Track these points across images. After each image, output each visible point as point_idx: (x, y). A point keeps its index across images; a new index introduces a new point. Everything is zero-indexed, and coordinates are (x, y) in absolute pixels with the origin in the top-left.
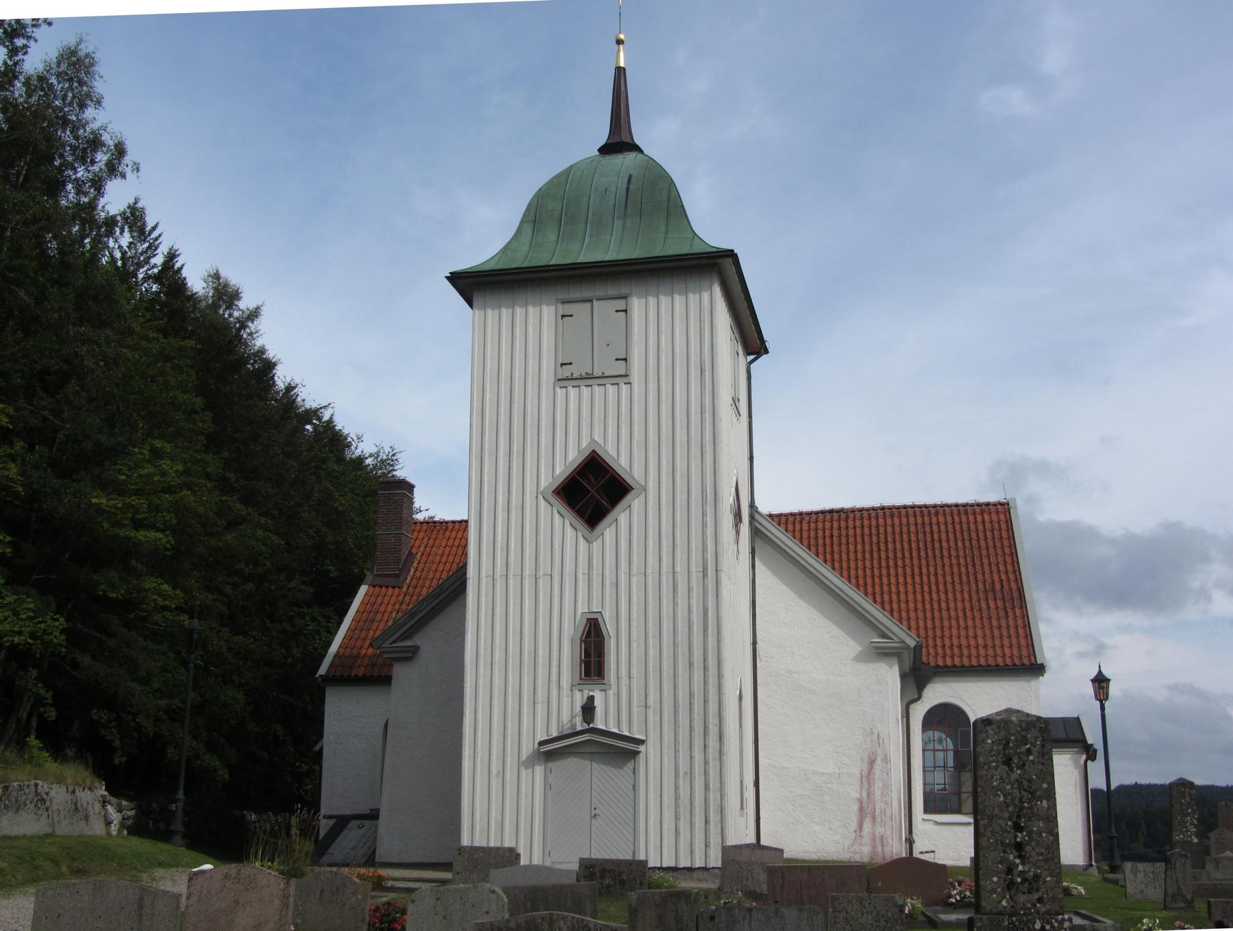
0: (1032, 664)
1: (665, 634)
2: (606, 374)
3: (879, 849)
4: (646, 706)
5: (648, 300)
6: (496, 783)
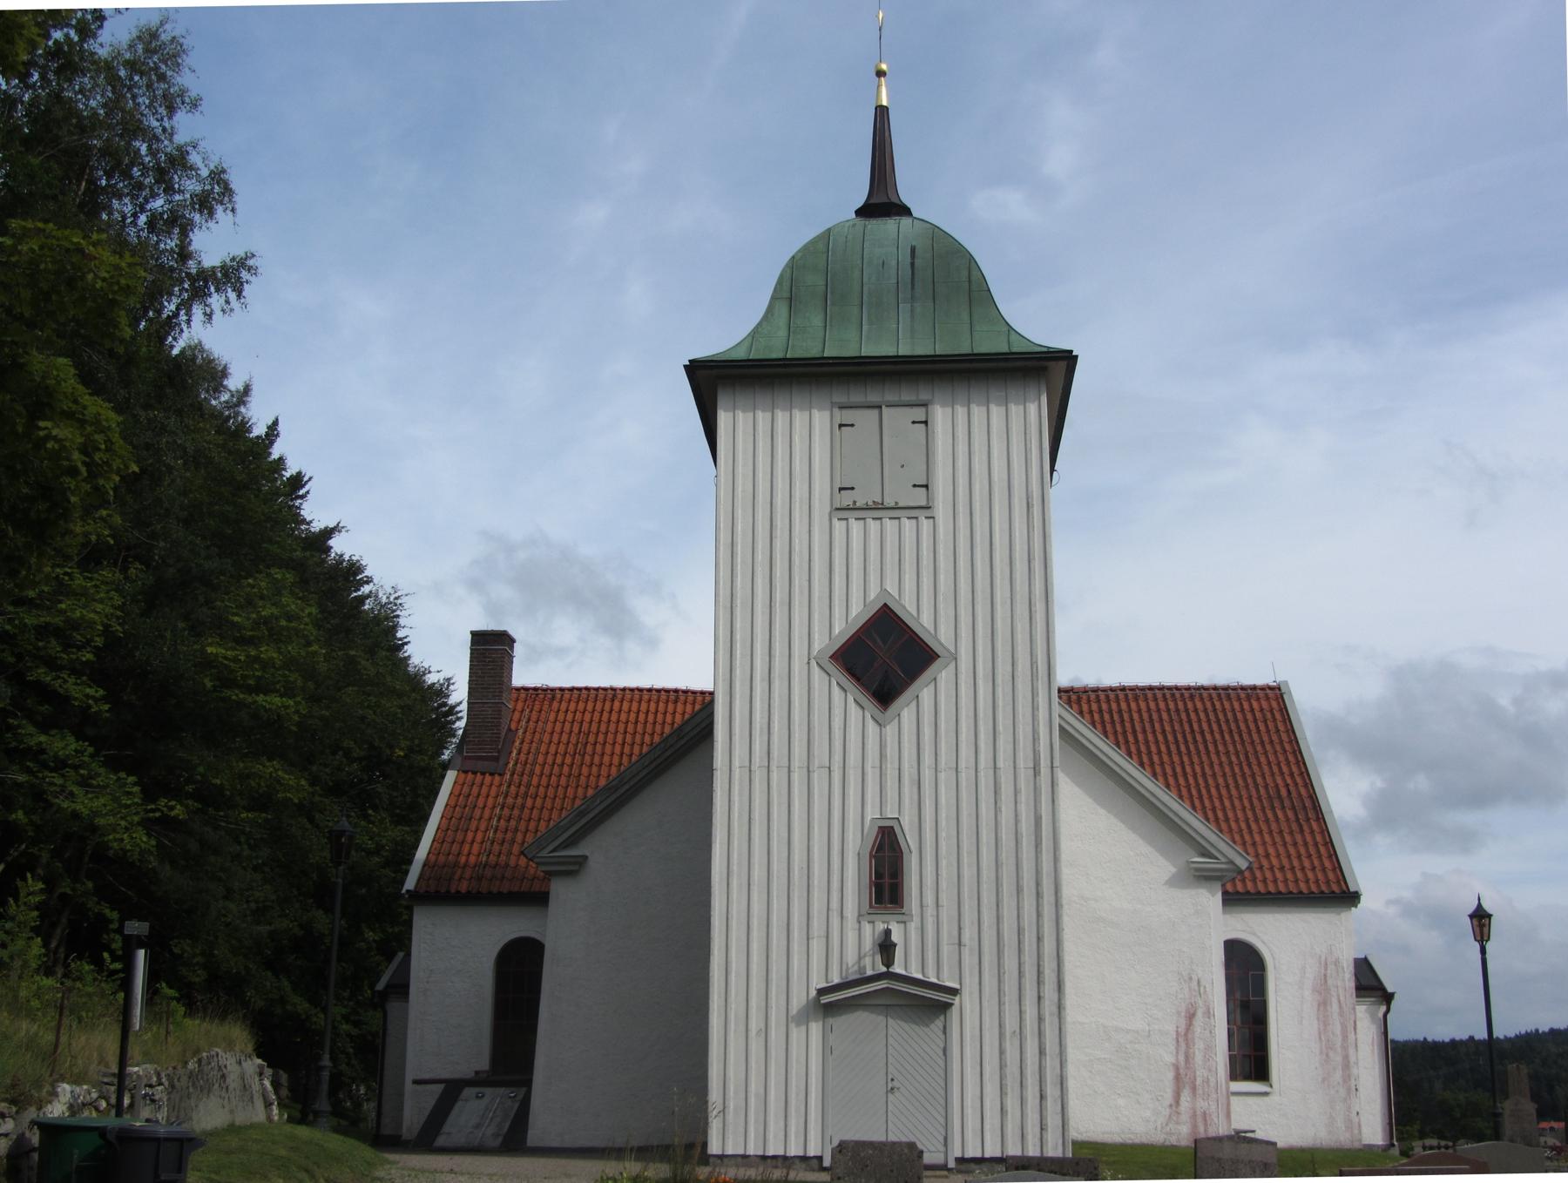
0: (1344, 892)
1: (984, 850)
2: (900, 505)
3: (1201, 1129)
4: (960, 944)
5: (955, 410)
6: (756, 1046)
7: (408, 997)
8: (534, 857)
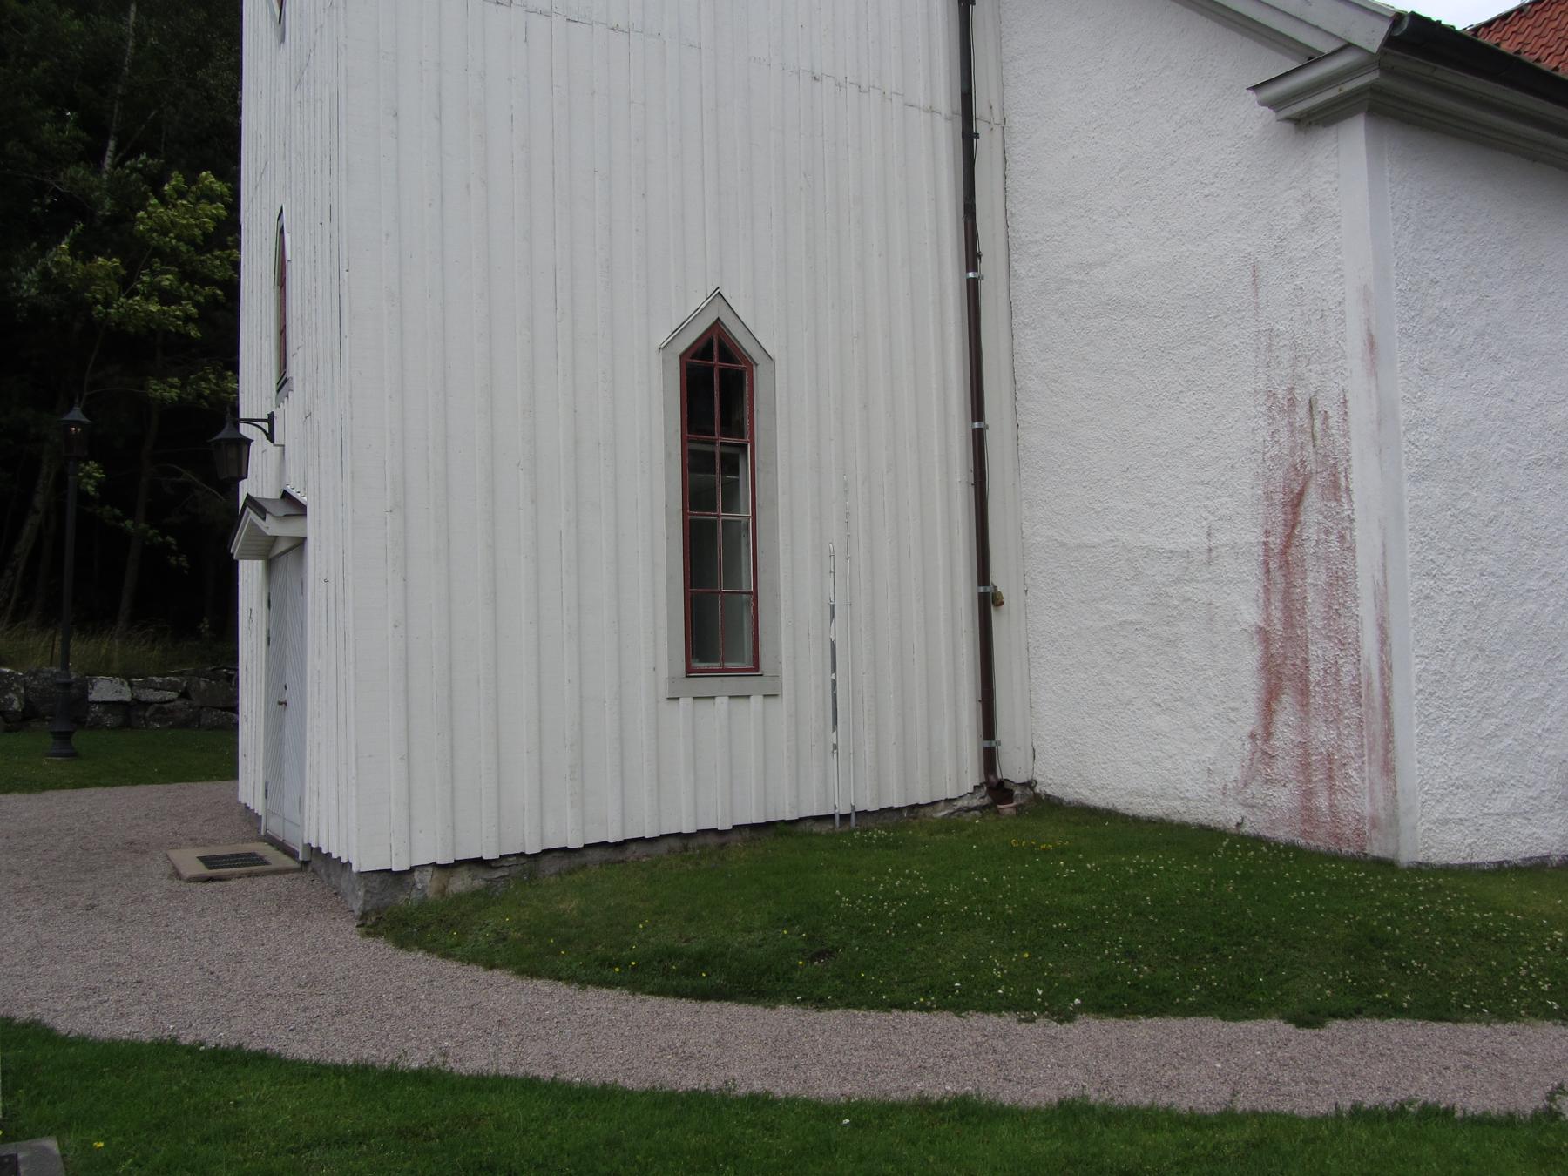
3: (1322, 802)
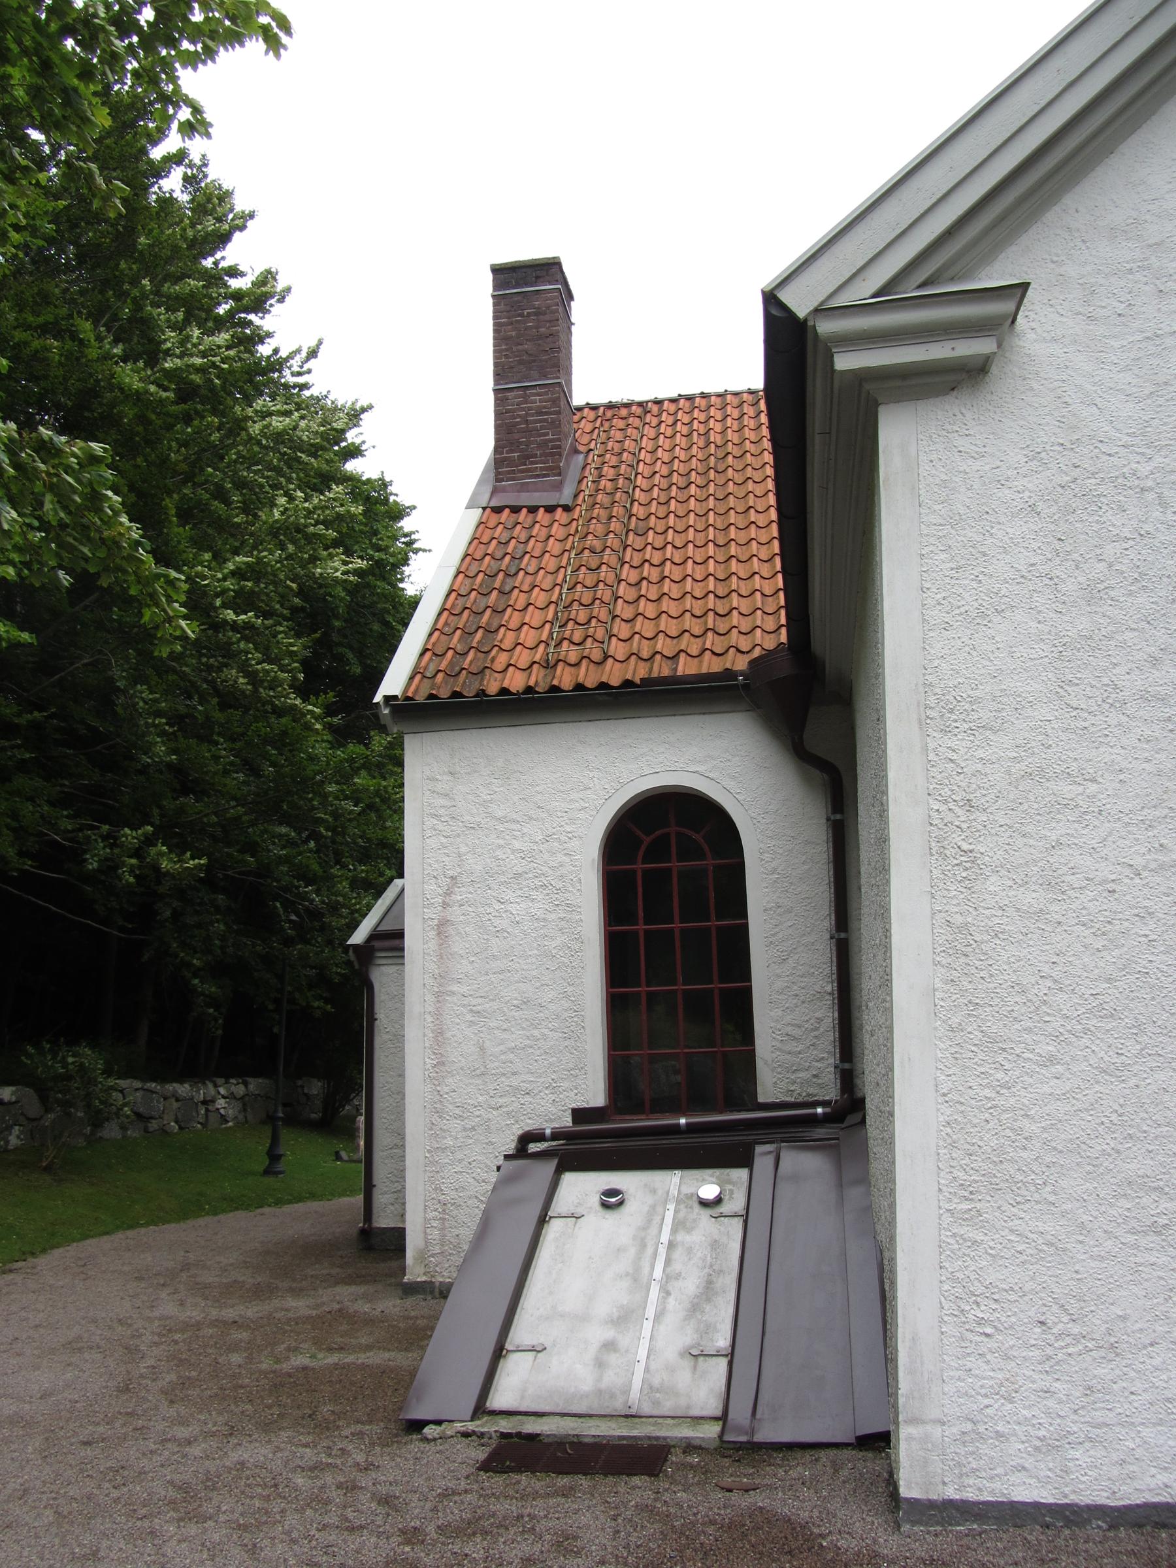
7: (403, 949)
8: (817, 311)
